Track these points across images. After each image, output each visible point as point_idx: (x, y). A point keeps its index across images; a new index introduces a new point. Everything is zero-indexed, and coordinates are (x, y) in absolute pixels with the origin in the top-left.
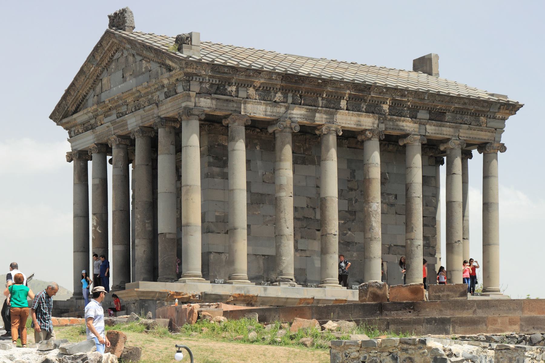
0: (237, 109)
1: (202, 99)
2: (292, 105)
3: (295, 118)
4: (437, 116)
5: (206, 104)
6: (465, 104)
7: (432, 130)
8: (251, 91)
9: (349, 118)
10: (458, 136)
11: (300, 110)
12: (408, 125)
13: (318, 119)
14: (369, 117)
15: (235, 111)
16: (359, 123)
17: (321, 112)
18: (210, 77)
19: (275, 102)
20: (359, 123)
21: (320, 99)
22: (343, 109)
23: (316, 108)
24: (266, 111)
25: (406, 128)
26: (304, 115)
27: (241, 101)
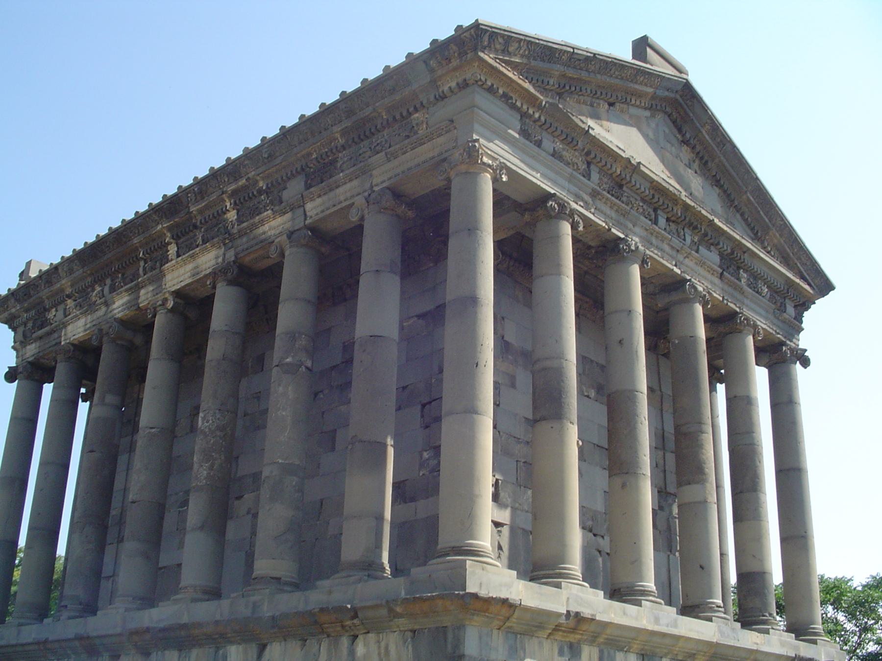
1: (28, 347)
4: (319, 174)
5: (31, 350)
6: (350, 113)
7: (314, 208)
8: (70, 303)
9: (181, 271)
12: (274, 225)
15: (56, 344)
21: (142, 263)
22: (172, 260)
25: (269, 233)
26: (129, 302)
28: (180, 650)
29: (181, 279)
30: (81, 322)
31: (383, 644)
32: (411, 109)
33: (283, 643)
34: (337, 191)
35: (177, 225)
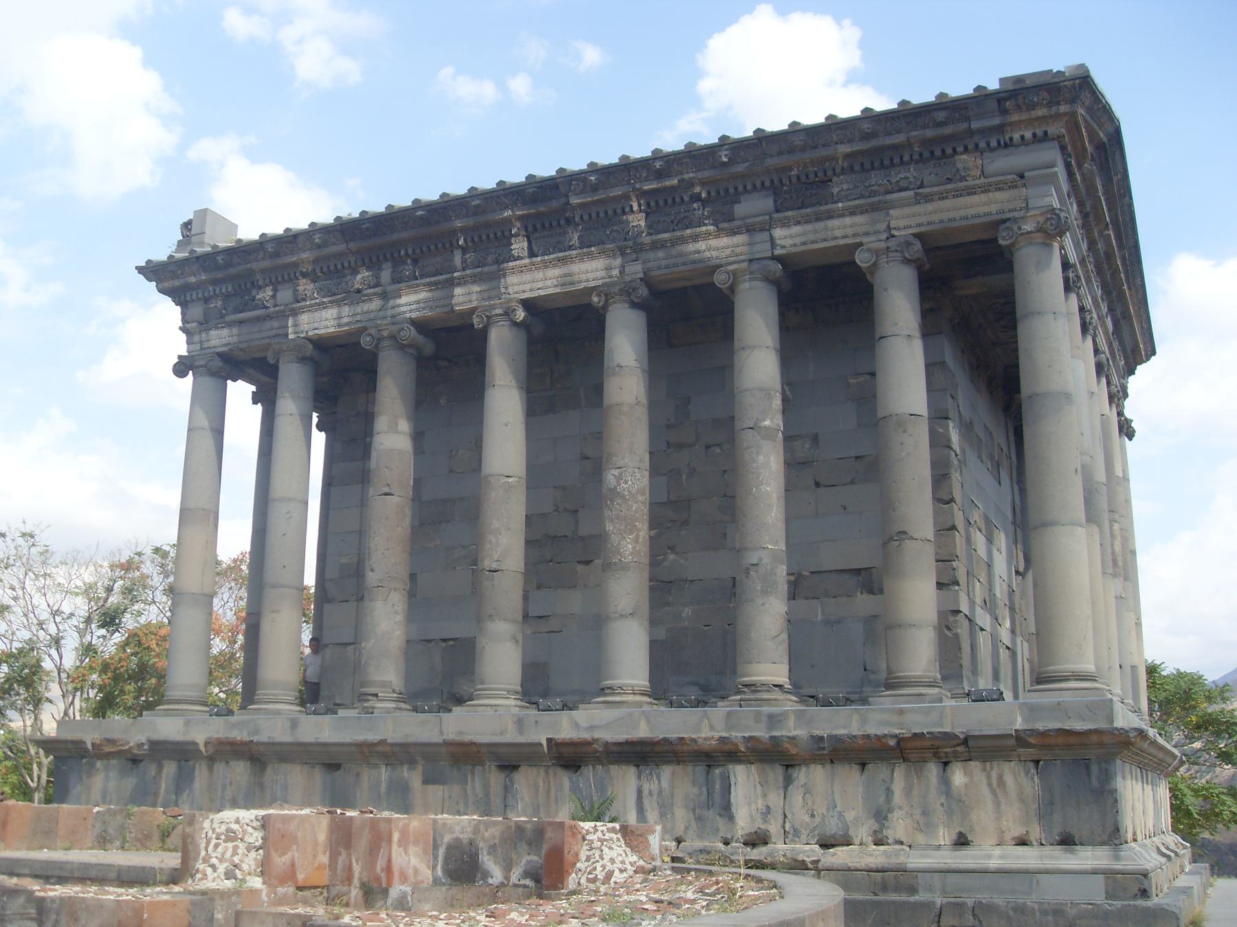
0: (279, 332)
1: (213, 333)
2: (390, 288)
3: (405, 312)
5: (220, 338)
6: (866, 136)
8: (305, 286)
9: (540, 275)
10: (889, 228)
11: (416, 292)
12: (715, 247)
13: (461, 299)
14: (591, 256)
15: (277, 336)
16: (567, 279)
17: (465, 283)
18: (215, 282)
19: (359, 291)
20: (567, 279)
22: (519, 258)
23: (448, 276)
24: (339, 318)
25: (707, 254)
26: (426, 301)
27: (283, 311)
28: (638, 766)
29: (540, 285)
30: (331, 313)
31: (994, 774)
32: (960, 149)
33: (828, 766)
34: (830, 223)
35: (537, 215)
